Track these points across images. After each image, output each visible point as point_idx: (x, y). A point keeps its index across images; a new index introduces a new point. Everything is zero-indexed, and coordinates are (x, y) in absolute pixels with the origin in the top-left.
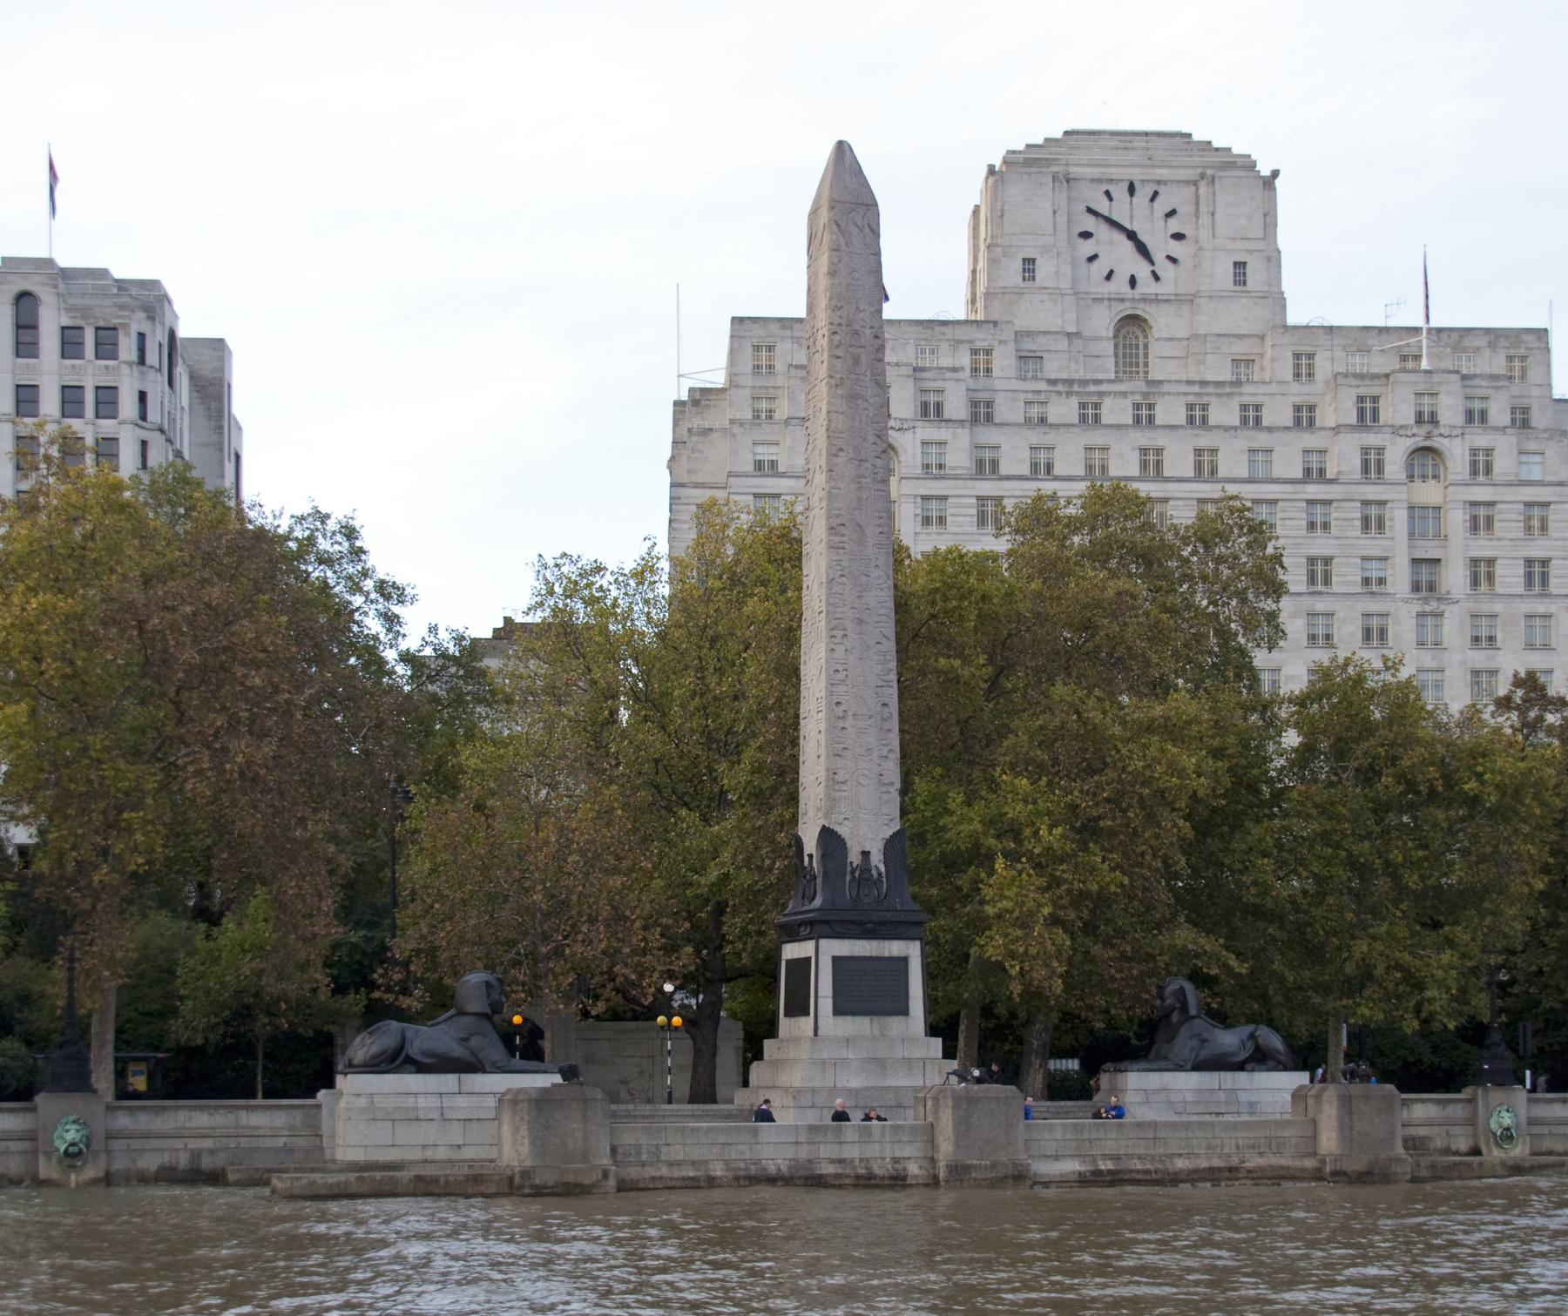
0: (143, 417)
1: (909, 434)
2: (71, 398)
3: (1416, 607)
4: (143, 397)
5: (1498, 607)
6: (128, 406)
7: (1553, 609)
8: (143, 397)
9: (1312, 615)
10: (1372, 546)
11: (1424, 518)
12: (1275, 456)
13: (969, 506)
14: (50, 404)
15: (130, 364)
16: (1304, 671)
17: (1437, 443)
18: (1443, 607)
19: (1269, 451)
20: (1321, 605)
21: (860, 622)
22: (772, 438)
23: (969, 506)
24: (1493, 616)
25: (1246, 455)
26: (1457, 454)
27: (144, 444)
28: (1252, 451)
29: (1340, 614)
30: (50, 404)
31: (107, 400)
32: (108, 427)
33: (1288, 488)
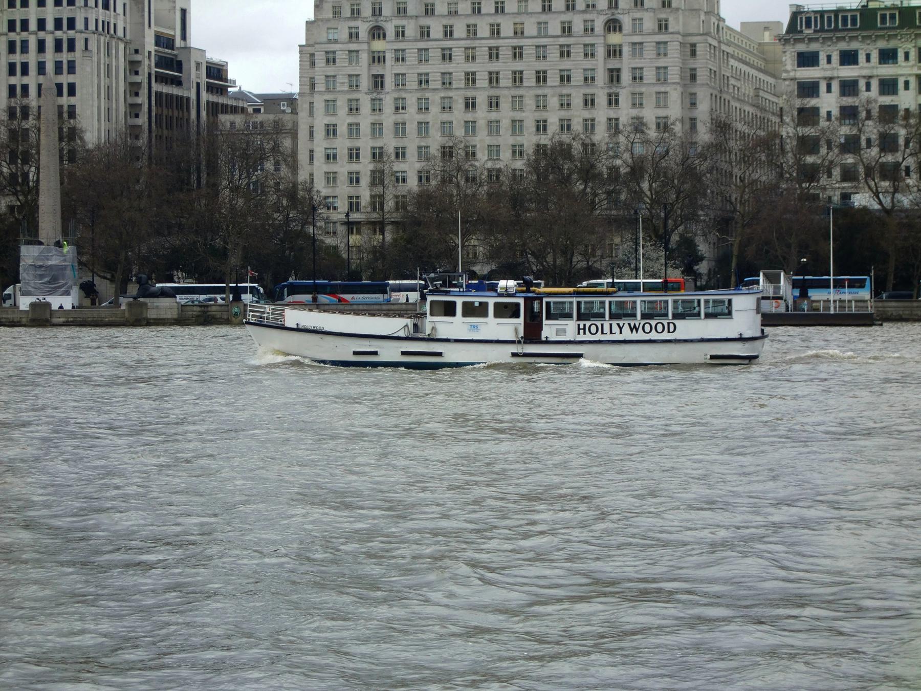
0: (86, 28)
1: (390, 22)
2: (58, 23)
3: (607, 91)
4: (86, 19)
5: (643, 89)
6: (80, 25)
7: (668, 89)
8: (86, 19)
9: (561, 96)
10: (588, 64)
11: (614, 52)
12: (549, 25)
13: (414, 53)
14: (50, 25)
15: (80, 8)
16: (557, 120)
17: (620, 17)
18: (618, 90)
19: (546, 23)
20: (565, 91)
21: (49, 190)
22: (335, 26)
23: (414, 53)
24: (641, 94)
25: (536, 25)
26: (626, 22)
27: (86, 40)
28: (539, 23)
29: (573, 95)
30: (50, 25)
31: (71, 23)
32: (71, 33)
33: (551, 39)
